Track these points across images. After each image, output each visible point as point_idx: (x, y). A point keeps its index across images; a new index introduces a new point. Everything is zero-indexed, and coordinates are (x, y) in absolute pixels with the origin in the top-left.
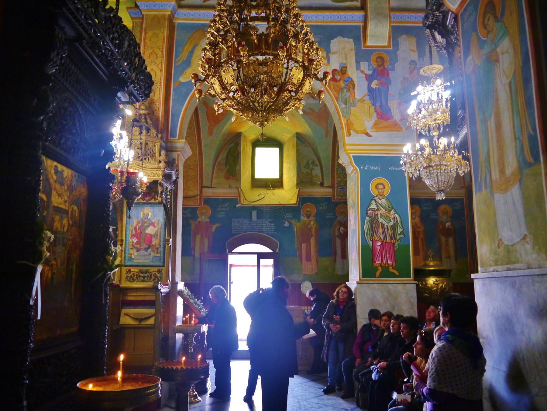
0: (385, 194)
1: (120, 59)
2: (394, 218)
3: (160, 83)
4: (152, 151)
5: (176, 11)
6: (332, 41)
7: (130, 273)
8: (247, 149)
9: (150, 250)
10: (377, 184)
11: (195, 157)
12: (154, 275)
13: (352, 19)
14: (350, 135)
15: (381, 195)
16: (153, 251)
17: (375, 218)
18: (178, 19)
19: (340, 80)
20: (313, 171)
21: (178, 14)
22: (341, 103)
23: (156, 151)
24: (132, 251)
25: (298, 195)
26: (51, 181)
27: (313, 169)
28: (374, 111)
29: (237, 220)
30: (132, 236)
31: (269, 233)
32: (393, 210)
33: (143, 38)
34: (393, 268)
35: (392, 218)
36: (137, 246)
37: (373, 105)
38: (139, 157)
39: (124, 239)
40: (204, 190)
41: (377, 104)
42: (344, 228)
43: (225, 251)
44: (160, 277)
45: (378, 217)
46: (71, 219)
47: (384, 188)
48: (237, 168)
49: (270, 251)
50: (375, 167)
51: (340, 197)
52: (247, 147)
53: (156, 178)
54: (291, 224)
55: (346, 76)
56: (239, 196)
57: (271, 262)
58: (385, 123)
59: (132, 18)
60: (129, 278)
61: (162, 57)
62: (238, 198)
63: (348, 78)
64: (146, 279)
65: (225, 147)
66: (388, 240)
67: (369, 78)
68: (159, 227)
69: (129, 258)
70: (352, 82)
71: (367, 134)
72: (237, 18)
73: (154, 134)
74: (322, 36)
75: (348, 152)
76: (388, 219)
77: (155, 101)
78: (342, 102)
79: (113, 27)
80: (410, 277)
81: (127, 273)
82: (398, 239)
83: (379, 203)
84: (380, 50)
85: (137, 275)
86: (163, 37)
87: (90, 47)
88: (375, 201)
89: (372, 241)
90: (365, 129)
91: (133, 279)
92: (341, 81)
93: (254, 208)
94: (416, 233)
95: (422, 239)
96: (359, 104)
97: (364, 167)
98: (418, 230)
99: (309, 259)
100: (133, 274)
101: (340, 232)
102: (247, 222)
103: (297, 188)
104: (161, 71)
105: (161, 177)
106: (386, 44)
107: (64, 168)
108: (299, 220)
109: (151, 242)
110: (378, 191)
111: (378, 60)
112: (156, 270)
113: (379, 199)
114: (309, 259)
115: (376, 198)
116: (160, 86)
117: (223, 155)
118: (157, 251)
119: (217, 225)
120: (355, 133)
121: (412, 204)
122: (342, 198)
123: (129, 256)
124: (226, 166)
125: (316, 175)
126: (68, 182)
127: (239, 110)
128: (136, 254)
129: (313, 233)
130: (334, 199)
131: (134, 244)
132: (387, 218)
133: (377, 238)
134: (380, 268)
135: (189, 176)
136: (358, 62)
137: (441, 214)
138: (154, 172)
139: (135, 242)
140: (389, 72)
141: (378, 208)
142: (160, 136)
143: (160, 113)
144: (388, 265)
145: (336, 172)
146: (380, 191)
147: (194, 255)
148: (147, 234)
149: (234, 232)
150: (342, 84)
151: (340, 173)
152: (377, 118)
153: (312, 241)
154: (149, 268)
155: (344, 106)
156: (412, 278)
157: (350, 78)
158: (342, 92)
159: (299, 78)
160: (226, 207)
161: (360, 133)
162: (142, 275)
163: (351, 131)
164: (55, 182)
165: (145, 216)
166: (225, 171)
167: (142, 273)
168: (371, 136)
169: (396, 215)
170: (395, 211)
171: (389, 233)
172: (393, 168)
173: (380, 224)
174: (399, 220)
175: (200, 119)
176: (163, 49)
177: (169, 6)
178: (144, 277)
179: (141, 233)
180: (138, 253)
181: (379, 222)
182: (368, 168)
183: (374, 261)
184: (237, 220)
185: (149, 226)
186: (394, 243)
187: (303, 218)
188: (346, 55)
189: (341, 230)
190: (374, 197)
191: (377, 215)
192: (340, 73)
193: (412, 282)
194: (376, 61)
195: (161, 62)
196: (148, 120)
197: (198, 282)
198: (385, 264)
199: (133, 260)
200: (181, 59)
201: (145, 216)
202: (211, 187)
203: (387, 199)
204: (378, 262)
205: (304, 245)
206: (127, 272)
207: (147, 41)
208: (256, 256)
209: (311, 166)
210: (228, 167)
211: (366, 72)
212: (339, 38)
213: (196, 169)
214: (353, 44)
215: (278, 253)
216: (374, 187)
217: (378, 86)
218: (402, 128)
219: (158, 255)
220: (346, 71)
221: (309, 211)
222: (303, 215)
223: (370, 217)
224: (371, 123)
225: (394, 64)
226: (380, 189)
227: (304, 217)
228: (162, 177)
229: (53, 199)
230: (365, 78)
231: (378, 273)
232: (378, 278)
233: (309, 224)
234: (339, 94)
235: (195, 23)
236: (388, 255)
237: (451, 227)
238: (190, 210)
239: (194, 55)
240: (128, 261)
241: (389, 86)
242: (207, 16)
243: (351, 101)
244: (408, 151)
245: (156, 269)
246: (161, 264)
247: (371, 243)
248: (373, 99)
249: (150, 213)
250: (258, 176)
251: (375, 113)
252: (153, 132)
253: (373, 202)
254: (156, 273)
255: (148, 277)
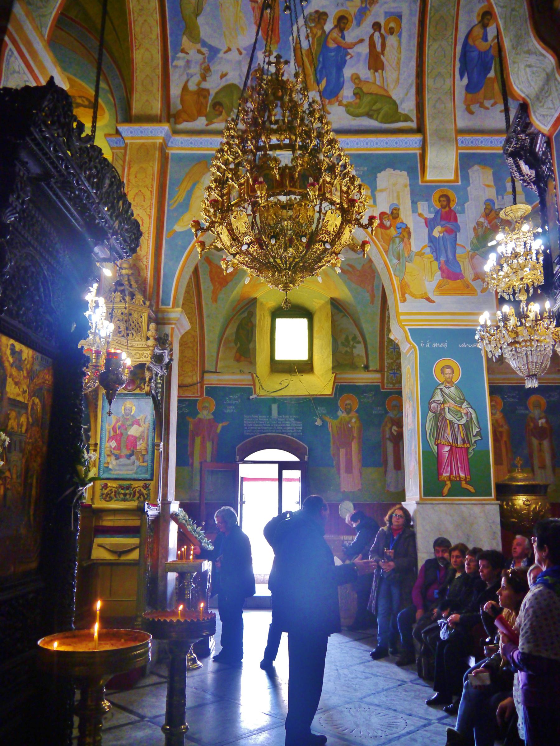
0: (453, 380)
1: (99, 203)
2: (467, 414)
3: (149, 233)
4: (138, 323)
5: (170, 138)
6: (379, 175)
7: (105, 489)
8: (264, 320)
9: (133, 457)
10: (443, 367)
11: (195, 331)
12: (138, 492)
13: (406, 145)
14: (405, 300)
15: (449, 382)
16: (137, 459)
17: (440, 414)
18: (172, 148)
19: (390, 226)
20: (354, 350)
21: (172, 143)
22: (393, 258)
23: (143, 324)
24: (109, 459)
25: (334, 382)
26: (7, 364)
27: (355, 347)
28: (437, 268)
29: (251, 417)
30: (109, 438)
31: (295, 434)
32: (465, 403)
33: (126, 174)
34: (467, 483)
35: (465, 414)
36: (116, 452)
37: (436, 259)
38: (120, 332)
39: (98, 442)
40: (207, 376)
41: (441, 259)
42: (397, 427)
43: (235, 458)
44: (147, 494)
45: (445, 413)
46: (32, 416)
47: (453, 372)
48: (251, 346)
49: (297, 459)
50: (440, 344)
51: (391, 386)
52: (264, 317)
53: (143, 360)
54: (325, 424)
55: (398, 220)
56: (254, 385)
57: (297, 474)
58: (452, 284)
59: (112, 148)
60: (104, 496)
61: (151, 199)
62: (253, 386)
63: (402, 224)
64: (128, 497)
65: (235, 318)
66: (459, 443)
67: (430, 224)
68: (147, 425)
69: (106, 469)
70: (407, 230)
71: (428, 299)
72: (252, 147)
73: (140, 301)
74: (366, 169)
75: (403, 323)
76: (459, 415)
77: (142, 257)
78: (394, 256)
79: (90, 160)
80: (491, 496)
81: (102, 489)
82: (473, 442)
83: (446, 394)
84: (444, 186)
85: (115, 492)
86: (152, 172)
87: (59, 188)
88: (441, 389)
89: (438, 445)
90: (426, 293)
91: (110, 497)
92: (392, 228)
93: (274, 400)
94: (498, 434)
95: (505, 442)
96: (417, 259)
97: (425, 343)
98: (501, 429)
99: (349, 469)
100: (111, 490)
101: (392, 433)
102: (265, 420)
103: (332, 373)
104: (150, 217)
105: (149, 359)
106: (452, 177)
107: (24, 348)
108: (336, 417)
109: (135, 446)
110: (444, 376)
111: (442, 199)
112: (142, 485)
113: (446, 387)
115: (442, 387)
116: (148, 237)
117: (231, 330)
118: (143, 458)
119: (225, 424)
120: (412, 298)
121: (491, 393)
122: (394, 386)
123: (106, 465)
124: (236, 344)
125: (358, 355)
126: (28, 366)
127: (255, 269)
128: (114, 462)
129: (355, 435)
130: (383, 388)
131: (112, 450)
132: (457, 413)
133: (443, 442)
134: (448, 483)
135: (185, 357)
136: (414, 202)
137: (531, 407)
138: (140, 352)
139: (113, 447)
140: (457, 215)
141: (444, 400)
142: (148, 303)
143: (149, 274)
144: (460, 478)
145: (386, 351)
146: (447, 376)
147: (192, 464)
148: (129, 436)
149: (248, 434)
150: (393, 232)
151: (392, 352)
152: (443, 278)
154: (132, 482)
155: (395, 261)
156: (493, 497)
157: (403, 223)
158: (394, 242)
159: (336, 225)
160: (235, 400)
161: (419, 298)
162: (122, 492)
163: (407, 295)
164: (12, 365)
165: (127, 411)
166: (234, 351)
167: (122, 489)
168: (434, 302)
169: (470, 410)
170: (469, 404)
171: (461, 434)
172: (464, 345)
173: (448, 421)
174: (474, 416)
175: (201, 281)
176: (152, 188)
177: (161, 132)
178: (125, 495)
179: (122, 434)
180: (118, 461)
181: (446, 419)
182: (431, 345)
183: (439, 474)
184: (251, 417)
185: (132, 425)
186: (467, 449)
187: (341, 414)
188: (398, 193)
189: (393, 431)
190: (440, 385)
191: (444, 408)
192: (391, 217)
193: (493, 502)
194: (440, 201)
195: (150, 206)
196: (133, 283)
197: (198, 502)
198: (456, 477)
199: (110, 472)
200: (177, 200)
201: (127, 411)
202: (216, 372)
203: (457, 387)
204: (446, 475)
205: (342, 451)
206: (103, 487)
207: (132, 177)
208: (276, 466)
209: (351, 343)
210: (239, 345)
211: (426, 216)
212: (389, 171)
213: (195, 349)
214: (408, 178)
215: (306, 462)
217: (442, 235)
218: (476, 290)
219: (145, 464)
220: (398, 214)
221: (350, 404)
222: (341, 410)
223: (434, 412)
224: (435, 283)
225: (463, 205)
226: (447, 374)
227: (343, 412)
228: (151, 358)
229: (8, 389)
230: (424, 224)
231: (446, 490)
232: (446, 496)
233: (349, 422)
234: (389, 246)
235: (195, 154)
236: (459, 465)
237: (545, 425)
238: (187, 403)
239: (193, 196)
240: (104, 472)
241: (458, 234)
242: (211, 144)
243: (406, 255)
244: (486, 322)
245: (141, 483)
246: (148, 476)
247: (436, 447)
248: (436, 251)
249: (134, 408)
250: (279, 356)
251: (439, 270)
252: (139, 298)
253: (438, 392)
254: (142, 489)
255: (130, 494)
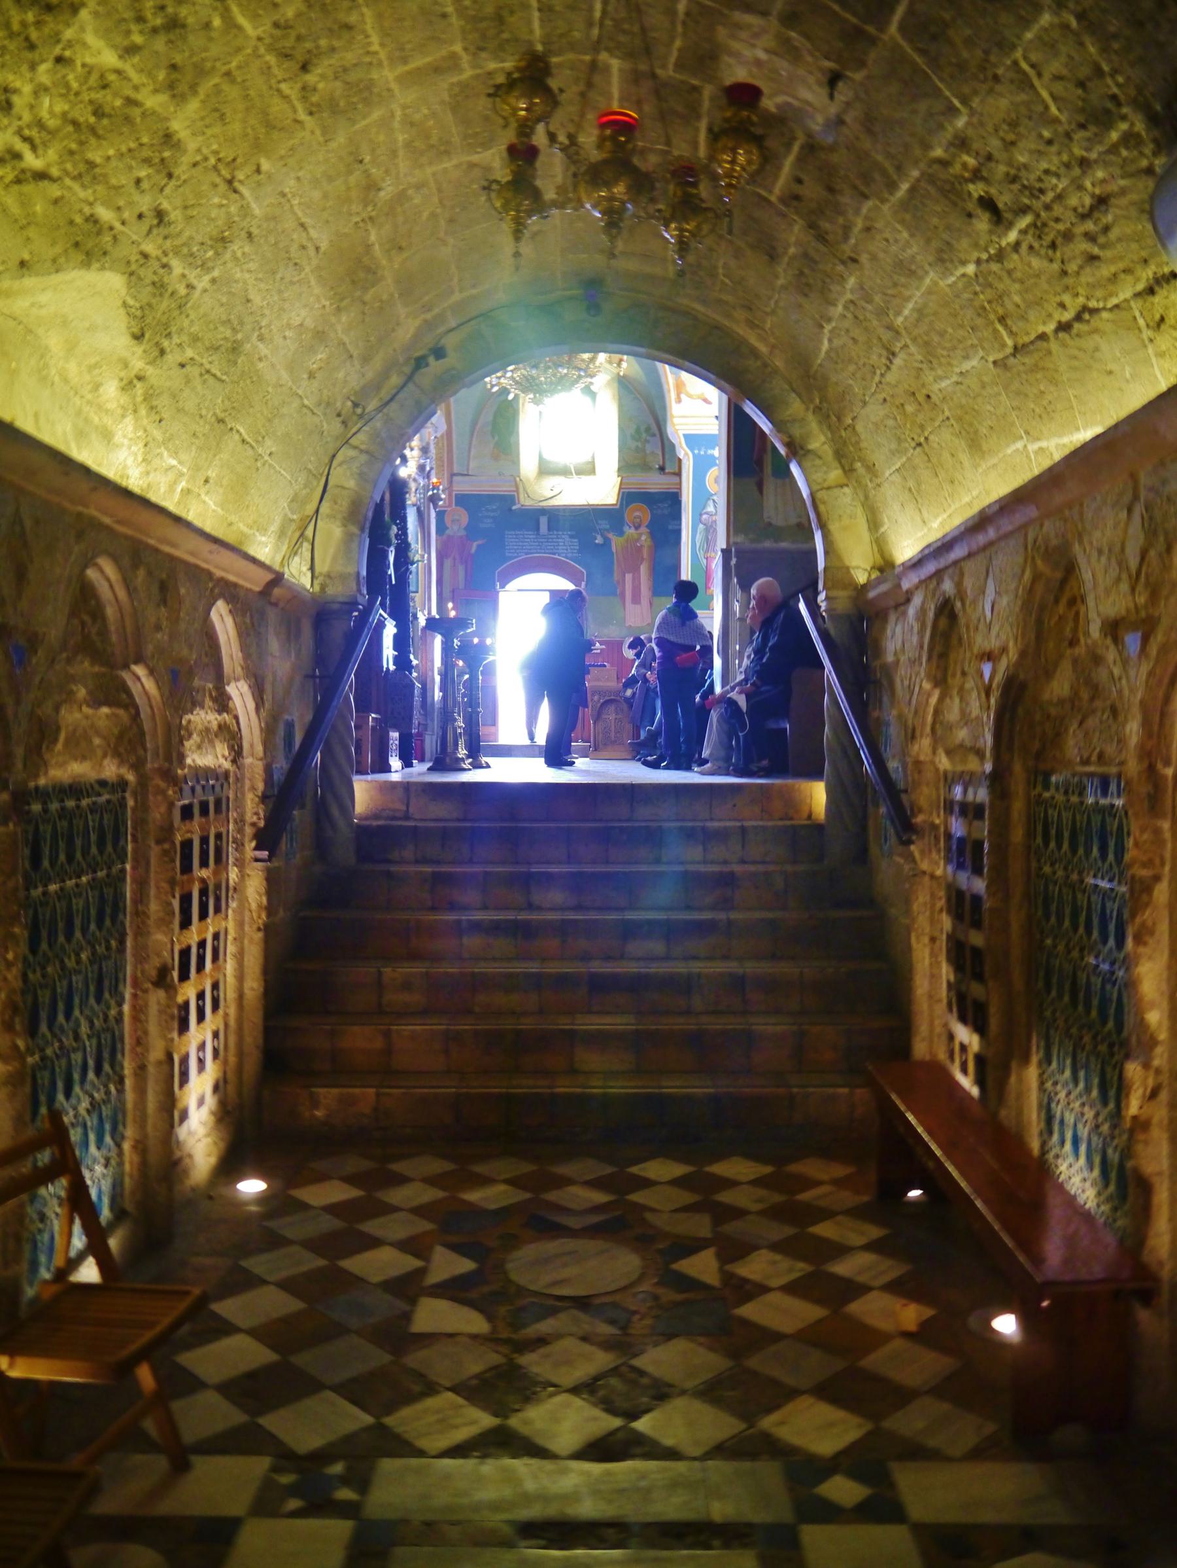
25: (620, 488)
54: (607, 541)
56: (517, 491)
93: (543, 511)
99: (636, 599)
108: (621, 533)
114: (636, 599)
115: (715, 498)
119: (480, 542)
153: (644, 569)
160: (493, 511)
163: (683, 396)
187: (630, 531)
205: (629, 577)
216: (712, 481)
221: (639, 517)
233: (638, 540)
253: (711, 503)
